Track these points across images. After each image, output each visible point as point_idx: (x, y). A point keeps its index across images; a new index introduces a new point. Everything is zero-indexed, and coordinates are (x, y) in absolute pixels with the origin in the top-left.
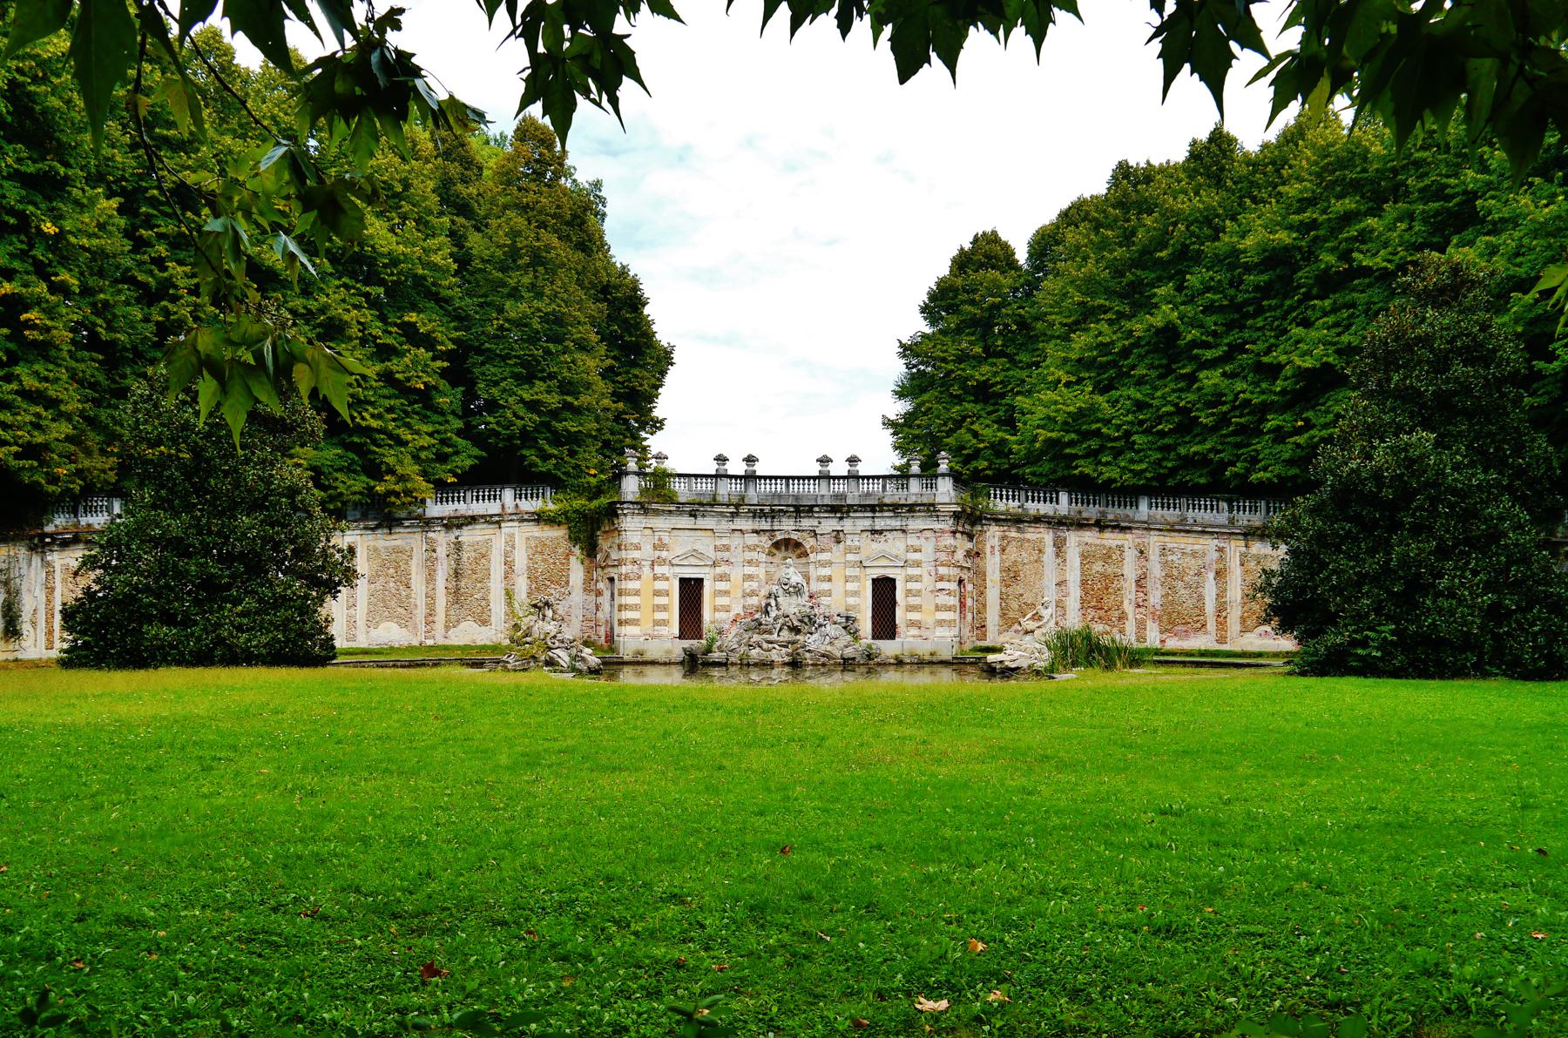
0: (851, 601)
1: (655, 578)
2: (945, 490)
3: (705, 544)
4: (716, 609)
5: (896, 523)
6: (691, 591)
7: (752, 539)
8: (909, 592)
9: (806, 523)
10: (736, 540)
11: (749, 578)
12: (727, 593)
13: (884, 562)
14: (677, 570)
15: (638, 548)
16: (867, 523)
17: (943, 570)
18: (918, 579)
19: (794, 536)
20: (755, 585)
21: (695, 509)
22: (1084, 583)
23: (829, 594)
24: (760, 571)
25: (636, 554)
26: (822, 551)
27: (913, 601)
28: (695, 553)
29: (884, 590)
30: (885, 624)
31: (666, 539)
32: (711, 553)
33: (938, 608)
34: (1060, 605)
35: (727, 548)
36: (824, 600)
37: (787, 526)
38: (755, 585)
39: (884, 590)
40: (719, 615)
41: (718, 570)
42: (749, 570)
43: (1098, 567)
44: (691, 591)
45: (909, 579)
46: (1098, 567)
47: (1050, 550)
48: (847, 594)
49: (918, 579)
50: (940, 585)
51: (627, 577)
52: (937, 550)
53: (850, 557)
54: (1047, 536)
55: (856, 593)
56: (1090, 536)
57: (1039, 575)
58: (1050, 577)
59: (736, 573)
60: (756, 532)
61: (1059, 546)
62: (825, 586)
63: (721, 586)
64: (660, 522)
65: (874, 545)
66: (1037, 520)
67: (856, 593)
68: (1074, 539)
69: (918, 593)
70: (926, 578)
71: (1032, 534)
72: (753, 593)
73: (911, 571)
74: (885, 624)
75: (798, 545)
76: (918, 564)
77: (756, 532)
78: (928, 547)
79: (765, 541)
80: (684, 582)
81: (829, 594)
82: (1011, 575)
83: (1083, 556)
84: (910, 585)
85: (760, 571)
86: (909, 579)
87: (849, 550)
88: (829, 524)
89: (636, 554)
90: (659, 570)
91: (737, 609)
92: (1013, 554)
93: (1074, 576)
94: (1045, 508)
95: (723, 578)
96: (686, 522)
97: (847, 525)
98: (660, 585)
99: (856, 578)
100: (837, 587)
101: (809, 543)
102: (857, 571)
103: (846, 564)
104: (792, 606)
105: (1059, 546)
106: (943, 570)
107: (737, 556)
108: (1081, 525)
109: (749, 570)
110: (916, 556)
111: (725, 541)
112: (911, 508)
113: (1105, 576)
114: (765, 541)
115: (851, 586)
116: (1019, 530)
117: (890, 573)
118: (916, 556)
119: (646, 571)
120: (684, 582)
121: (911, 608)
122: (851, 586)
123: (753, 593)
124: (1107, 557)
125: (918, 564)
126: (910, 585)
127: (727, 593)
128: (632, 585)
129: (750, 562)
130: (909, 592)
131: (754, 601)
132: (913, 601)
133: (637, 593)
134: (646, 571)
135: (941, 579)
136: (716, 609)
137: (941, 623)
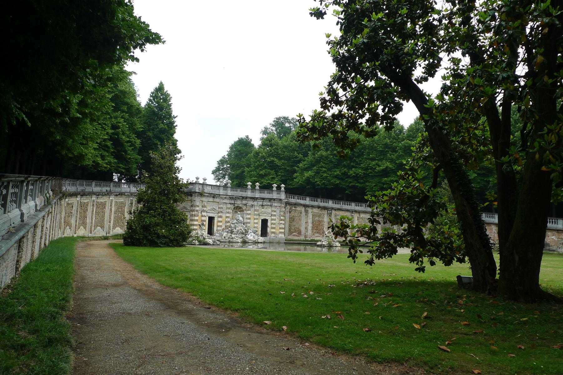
0: (256, 225)
1: (202, 216)
2: (283, 196)
3: (216, 206)
4: (218, 226)
5: (269, 204)
6: (211, 219)
7: (229, 206)
8: (272, 224)
9: (244, 202)
10: (224, 206)
11: (227, 217)
12: (221, 222)
13: (265, 215)
14: (208, 214)
15: (198, 207)
16: (261, 203)
17: (282, 218)
18: (275, 220)
19: (240, 206)
20: (229, 219)
21: (214, 196)
22: (313, 223)
23: (249, 223)
24: (230, 215)
25: (197, 209)
26: (248, 210)
27: (273, 226)
28: (214, 209)
29: (264, 223)
30: (264, 233)
31: (206, 204)
32: (217, 209)
33: (280, 228)
34: (306, 228)
35: (222, 208)
36: (248, 225)
37: (239, 202)
38: (229, 219)
39: (264, 223)
40: (219, 228)
41: (219, 214)
42: (228, 215)
43: (317, 218)
44: (211, 219)
45: (272, 220)
46: (317, 218)
47: (303, 213)
48: (254, 223)
49: (275, 220)
50: (281, 222)
51: (195, 216)
52: (280, 212)
53: (256, 213)
54: (303, 209)
55: (257, 223)
56: (316, 210)
57: (300, 220)
58: (303, 221)
59: (224, 216)
60: (230, 203)
61: (306, 212)
62: (249, 221)
63: (220, 219)
64: (204, 199)
65: (263, 210)
66: (301, 205)
67: (257, 223)
68: (310, 210)
69: (274, 224)
70: (277, 220)
71: (298, 209)
72: (229, 222)
73: (273, 218)
74: (264, 233)
75: (240, 208)
76: (275, 215)
77: (230, 203)
78: (278, 211)
79: (232, 207)
80: (209, 217)
81: (249, 223)
82: (292, 220)
83: (313, 215)
84: (272, 222)
85: (230, 215)
86: (272, 220)
87: (255, 210)
88: (250, 203)
89: (197, 209)
90: (204, 214)
91: (224, 227)
92: (293, 214)
93: (310, 221)
94: (302, 202)
95: (221, 217)
96: (211, 199)
97: (255, 203)
98: (203, 218)
99: (257, 219)
100: (252, 221)
101: (244, 208)
102: (257, 217)
103: (255, 215)
104: (240, 227)
105: (306, 212)
106: (282, 218)
107: (225, 210)
108: (313, 207)
109: (228, 215)
110: (275, 213)
111: (222, 206)
112: (274, 199)
113: (319, 221)
114: (232, 207)
115: (256, 221)
116: (295, 207)
117: (267, 218)
118: (275, 213)
119: (200, 214)
120: (209, 217)
121: (272, 228)
122: (256, 221)
123: (229, 222)
124: (319, 216)
125: (275, 215)
126: (272, 222)
127: (221, 222)
128: (196, 218)
129: (228, 213)
130: (272, 224)
131: (228, 224)
132: (273, 226)
133: (197, 220)
134: (200, 214)
135: (282, 220)
136: (218, 226)
137: (281, 233)
